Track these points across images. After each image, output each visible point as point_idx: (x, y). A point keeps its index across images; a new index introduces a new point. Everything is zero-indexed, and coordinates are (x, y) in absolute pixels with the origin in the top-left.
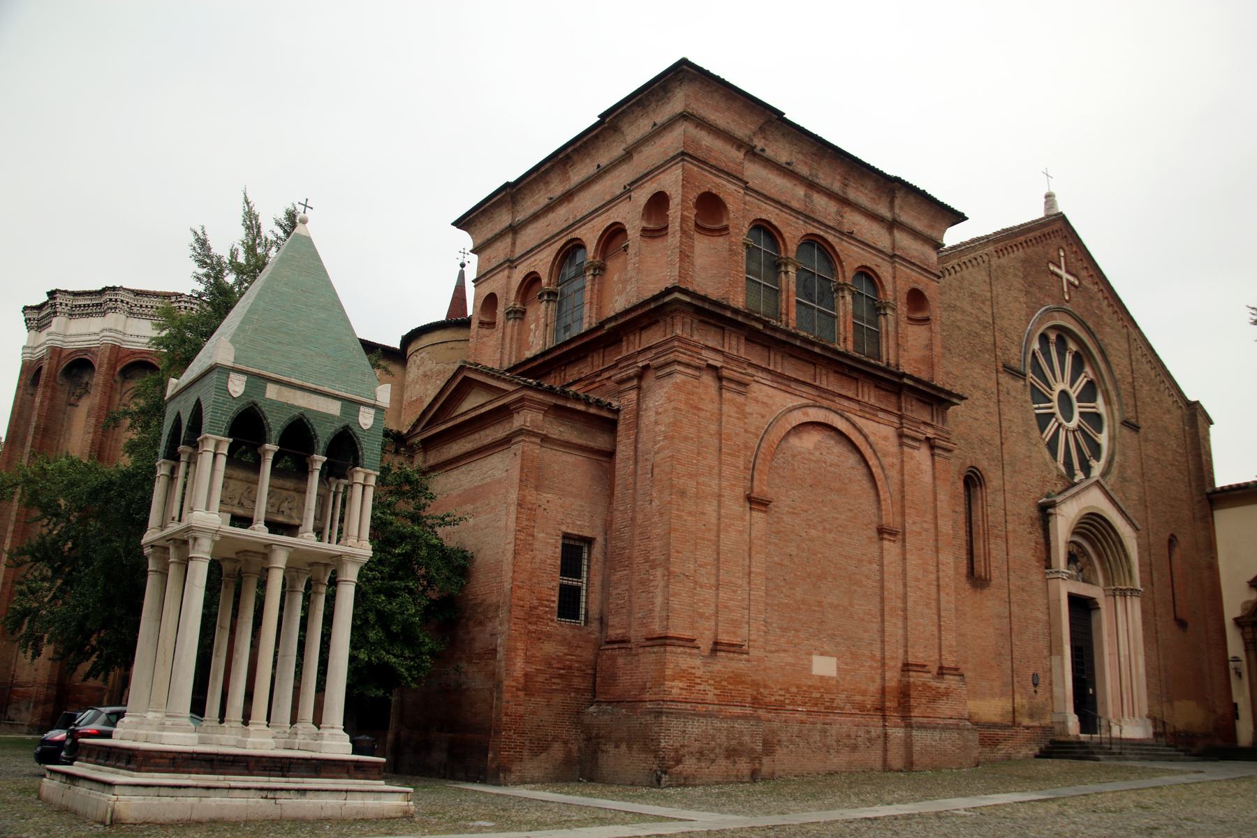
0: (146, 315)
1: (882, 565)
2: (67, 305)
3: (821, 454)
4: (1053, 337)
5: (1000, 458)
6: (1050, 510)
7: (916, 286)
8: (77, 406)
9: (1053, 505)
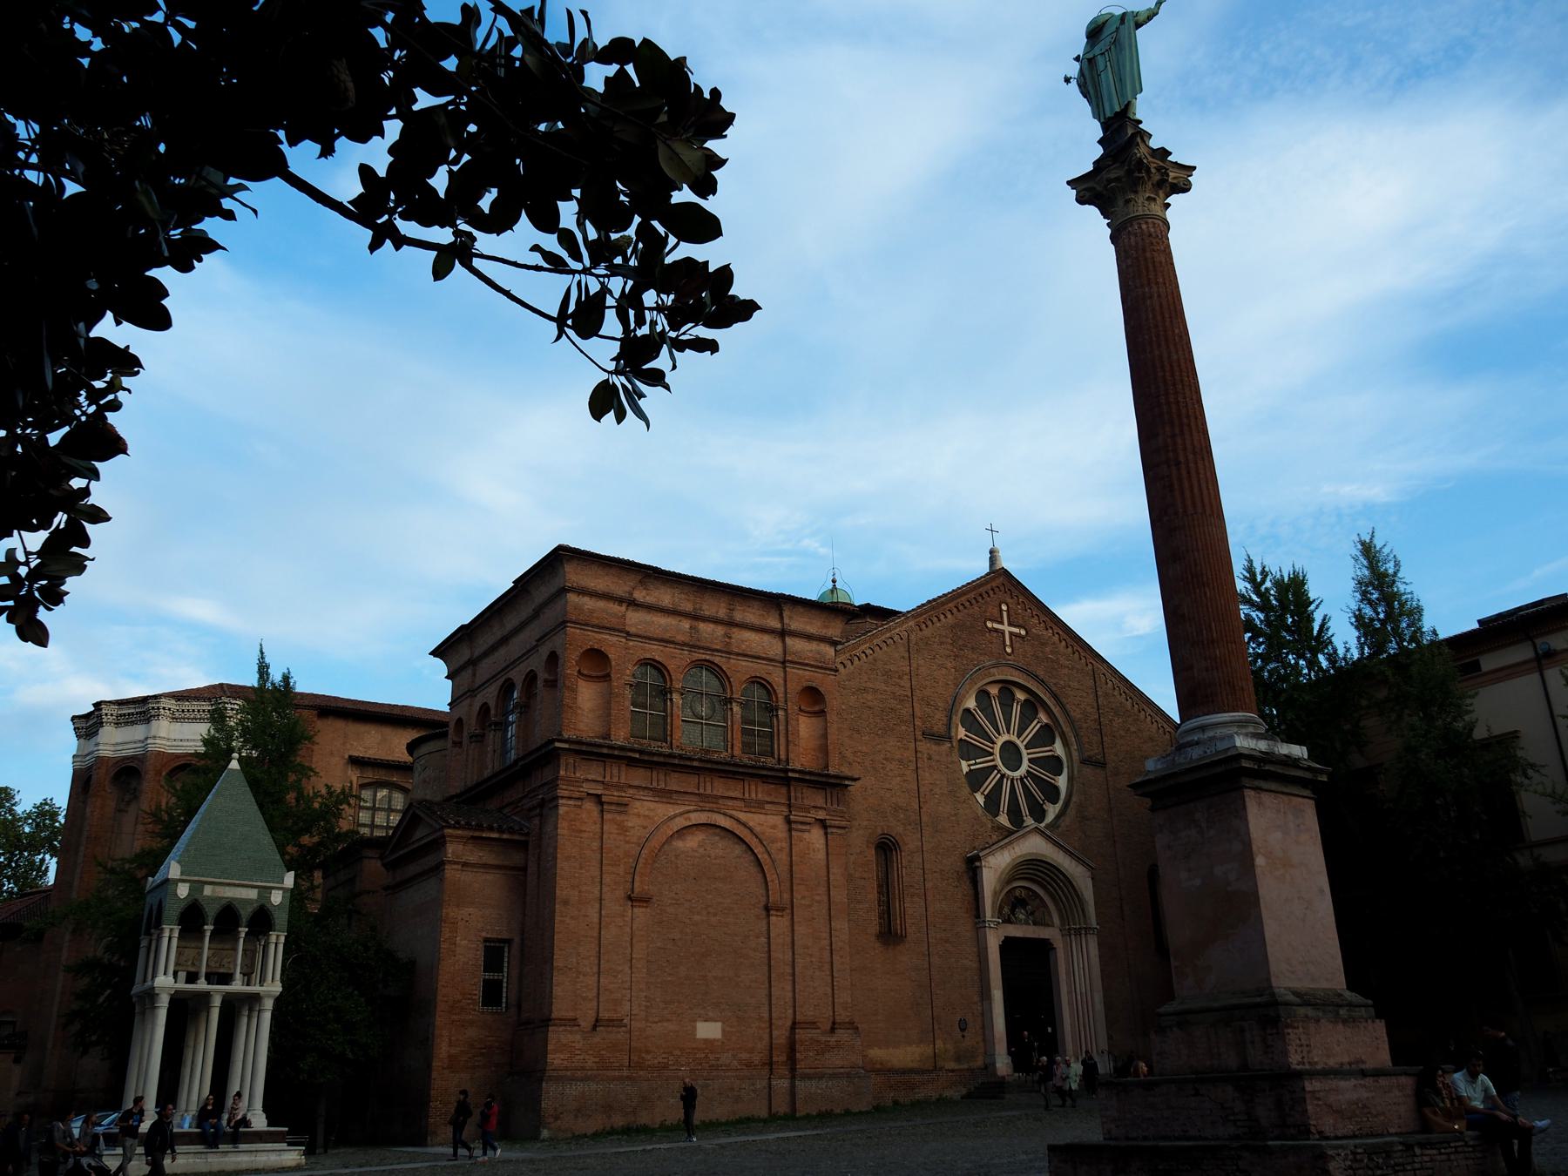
0: (188, 719)
1: (769, 938)
2: (112, 715)
3: (705, 850)
4: (994, 691)
5: (919, 822)
6: (977, 864)
7: (810, 684)
9: (978, 858)
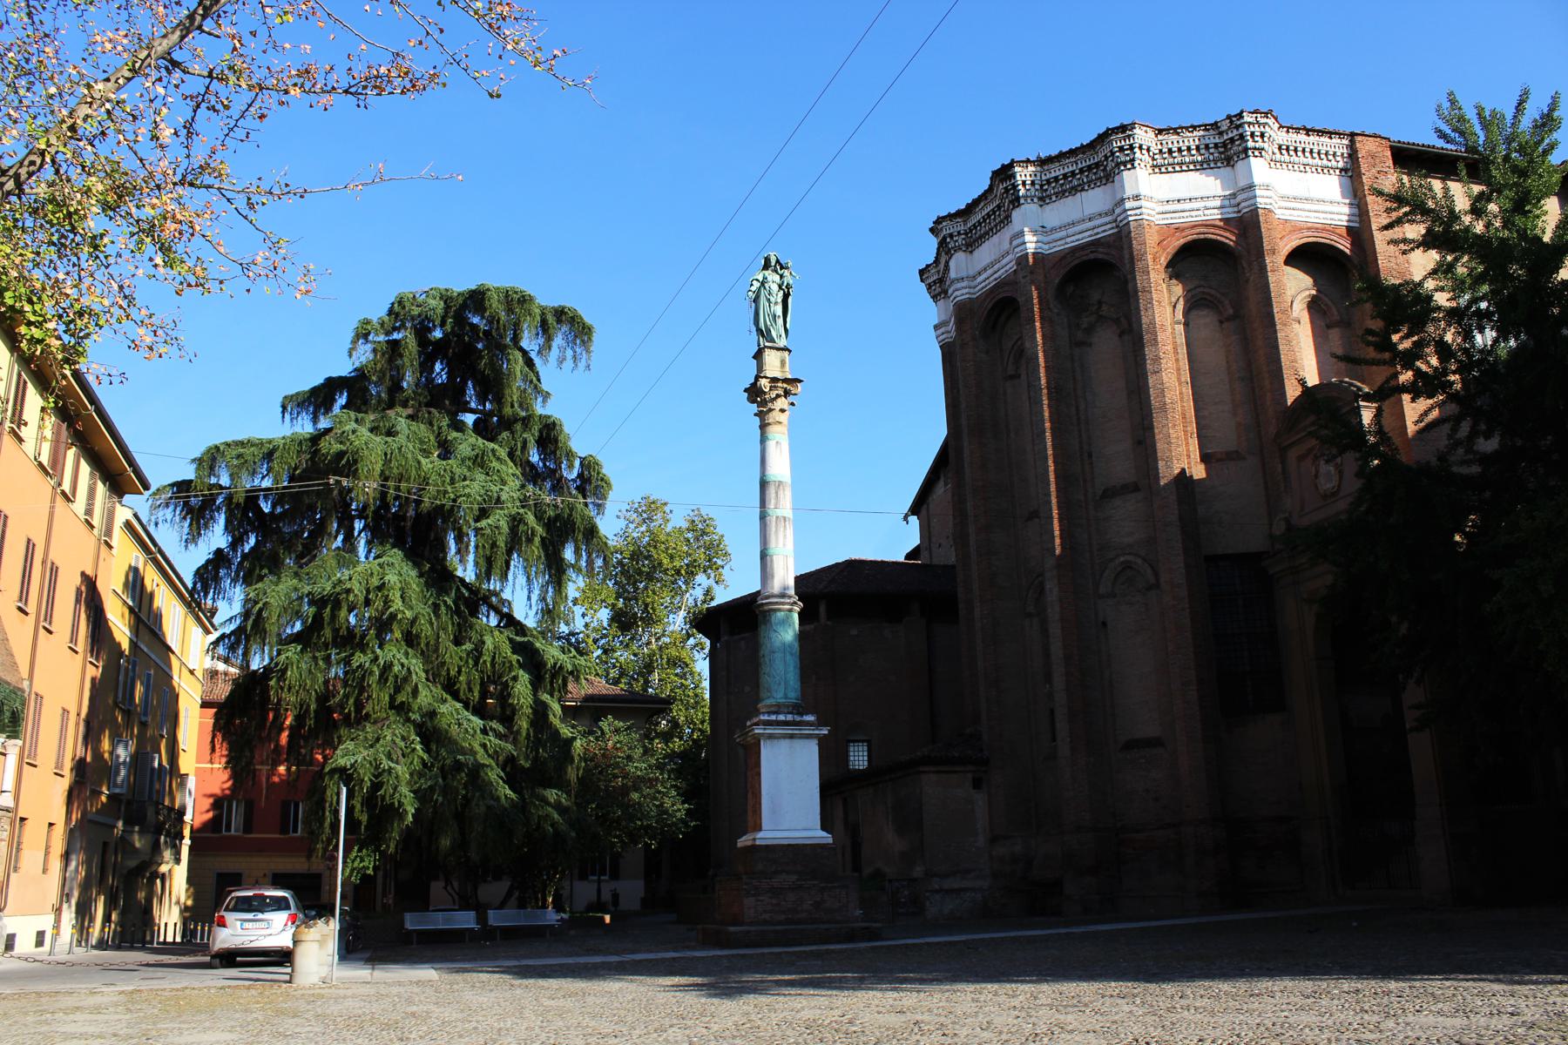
8: (1090, 345)
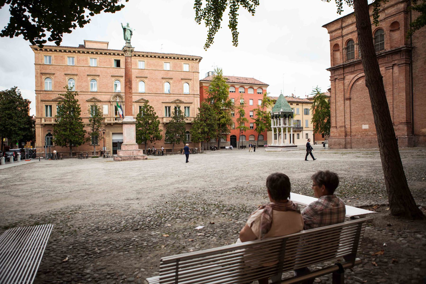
7: (394, 21)
